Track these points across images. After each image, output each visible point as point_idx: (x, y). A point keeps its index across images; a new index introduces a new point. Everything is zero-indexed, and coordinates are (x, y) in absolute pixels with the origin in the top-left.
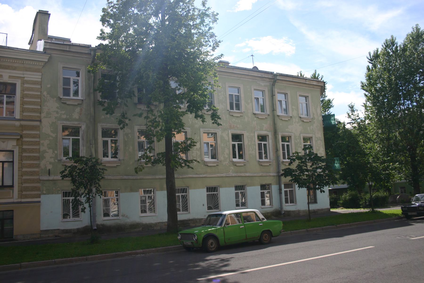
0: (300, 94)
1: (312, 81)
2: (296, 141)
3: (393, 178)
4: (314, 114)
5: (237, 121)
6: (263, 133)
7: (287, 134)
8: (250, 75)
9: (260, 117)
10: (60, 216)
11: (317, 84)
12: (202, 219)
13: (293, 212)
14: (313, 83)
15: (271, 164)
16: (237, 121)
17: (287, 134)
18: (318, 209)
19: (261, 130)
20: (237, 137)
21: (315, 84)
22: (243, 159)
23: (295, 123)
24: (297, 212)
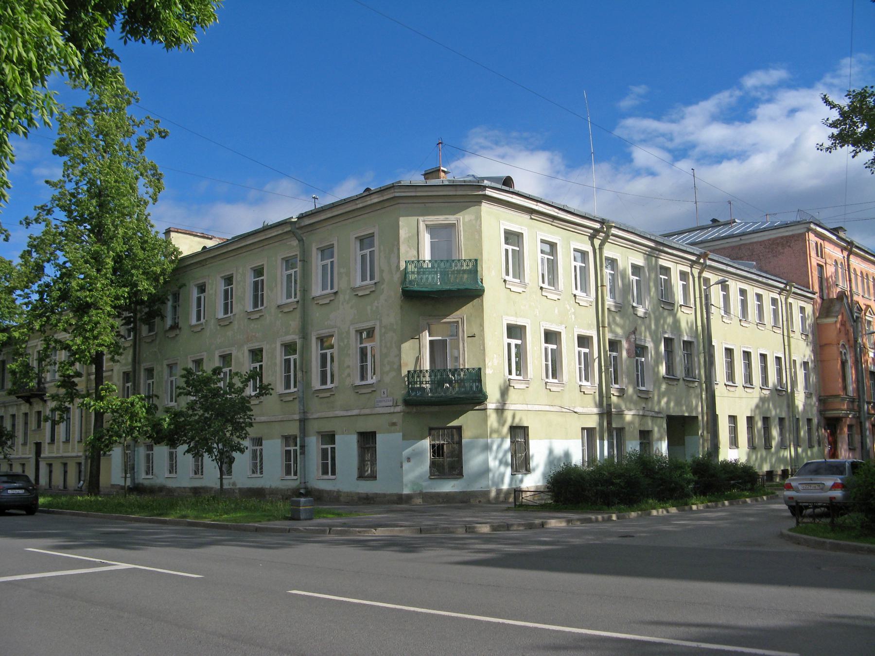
0: (356, 236)
1: (368, 198)
2: (342, 344)
3: (171, 416)
4: (382, 271)
5: (256, 326)
6: (289, 338)
7: (327, 331)
8: (267, 237)
9: (321, 302)
10: (54, 465)
11: (381, 199)
12: (212, 488)
13: (329, 492)
14: (371, 200)
15: (295, 397)
16: (256, 326)
17: (327, 331)
18: (376, 494)
19: (287, 333)
20: (515, 331)
21: (376, 200)
22: (556, 378)
23: (343, 304)
24: (335, 494)
